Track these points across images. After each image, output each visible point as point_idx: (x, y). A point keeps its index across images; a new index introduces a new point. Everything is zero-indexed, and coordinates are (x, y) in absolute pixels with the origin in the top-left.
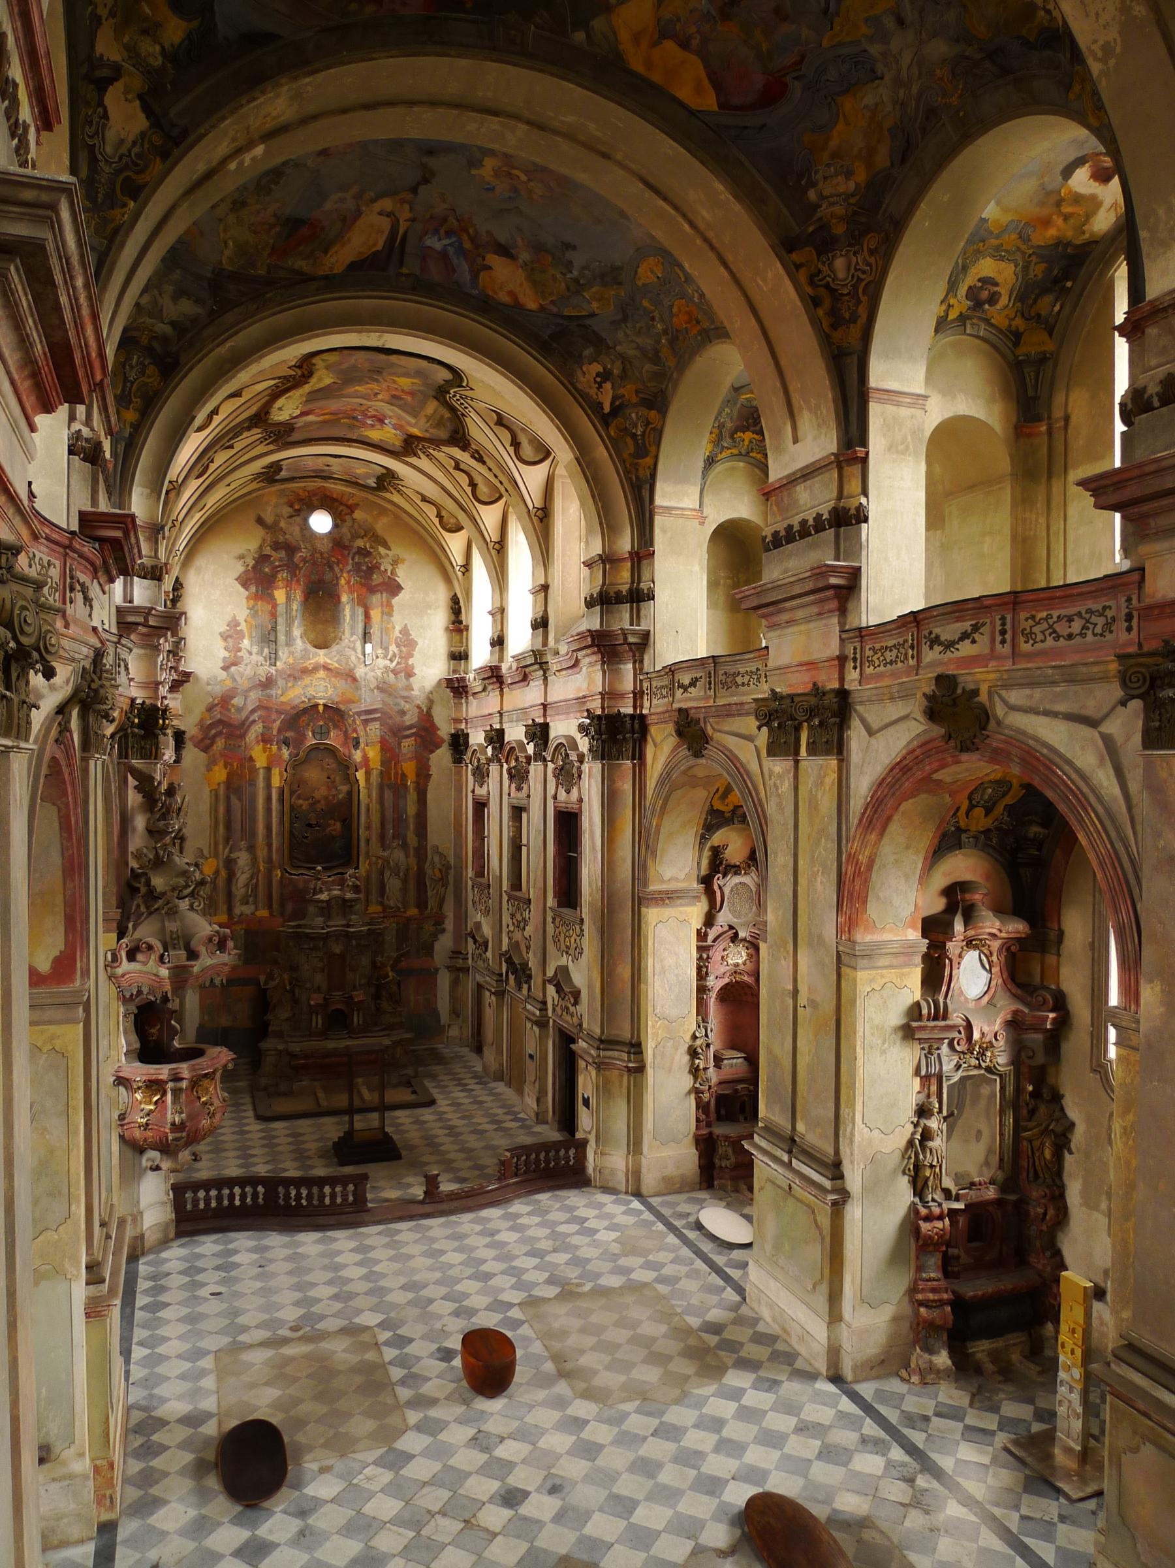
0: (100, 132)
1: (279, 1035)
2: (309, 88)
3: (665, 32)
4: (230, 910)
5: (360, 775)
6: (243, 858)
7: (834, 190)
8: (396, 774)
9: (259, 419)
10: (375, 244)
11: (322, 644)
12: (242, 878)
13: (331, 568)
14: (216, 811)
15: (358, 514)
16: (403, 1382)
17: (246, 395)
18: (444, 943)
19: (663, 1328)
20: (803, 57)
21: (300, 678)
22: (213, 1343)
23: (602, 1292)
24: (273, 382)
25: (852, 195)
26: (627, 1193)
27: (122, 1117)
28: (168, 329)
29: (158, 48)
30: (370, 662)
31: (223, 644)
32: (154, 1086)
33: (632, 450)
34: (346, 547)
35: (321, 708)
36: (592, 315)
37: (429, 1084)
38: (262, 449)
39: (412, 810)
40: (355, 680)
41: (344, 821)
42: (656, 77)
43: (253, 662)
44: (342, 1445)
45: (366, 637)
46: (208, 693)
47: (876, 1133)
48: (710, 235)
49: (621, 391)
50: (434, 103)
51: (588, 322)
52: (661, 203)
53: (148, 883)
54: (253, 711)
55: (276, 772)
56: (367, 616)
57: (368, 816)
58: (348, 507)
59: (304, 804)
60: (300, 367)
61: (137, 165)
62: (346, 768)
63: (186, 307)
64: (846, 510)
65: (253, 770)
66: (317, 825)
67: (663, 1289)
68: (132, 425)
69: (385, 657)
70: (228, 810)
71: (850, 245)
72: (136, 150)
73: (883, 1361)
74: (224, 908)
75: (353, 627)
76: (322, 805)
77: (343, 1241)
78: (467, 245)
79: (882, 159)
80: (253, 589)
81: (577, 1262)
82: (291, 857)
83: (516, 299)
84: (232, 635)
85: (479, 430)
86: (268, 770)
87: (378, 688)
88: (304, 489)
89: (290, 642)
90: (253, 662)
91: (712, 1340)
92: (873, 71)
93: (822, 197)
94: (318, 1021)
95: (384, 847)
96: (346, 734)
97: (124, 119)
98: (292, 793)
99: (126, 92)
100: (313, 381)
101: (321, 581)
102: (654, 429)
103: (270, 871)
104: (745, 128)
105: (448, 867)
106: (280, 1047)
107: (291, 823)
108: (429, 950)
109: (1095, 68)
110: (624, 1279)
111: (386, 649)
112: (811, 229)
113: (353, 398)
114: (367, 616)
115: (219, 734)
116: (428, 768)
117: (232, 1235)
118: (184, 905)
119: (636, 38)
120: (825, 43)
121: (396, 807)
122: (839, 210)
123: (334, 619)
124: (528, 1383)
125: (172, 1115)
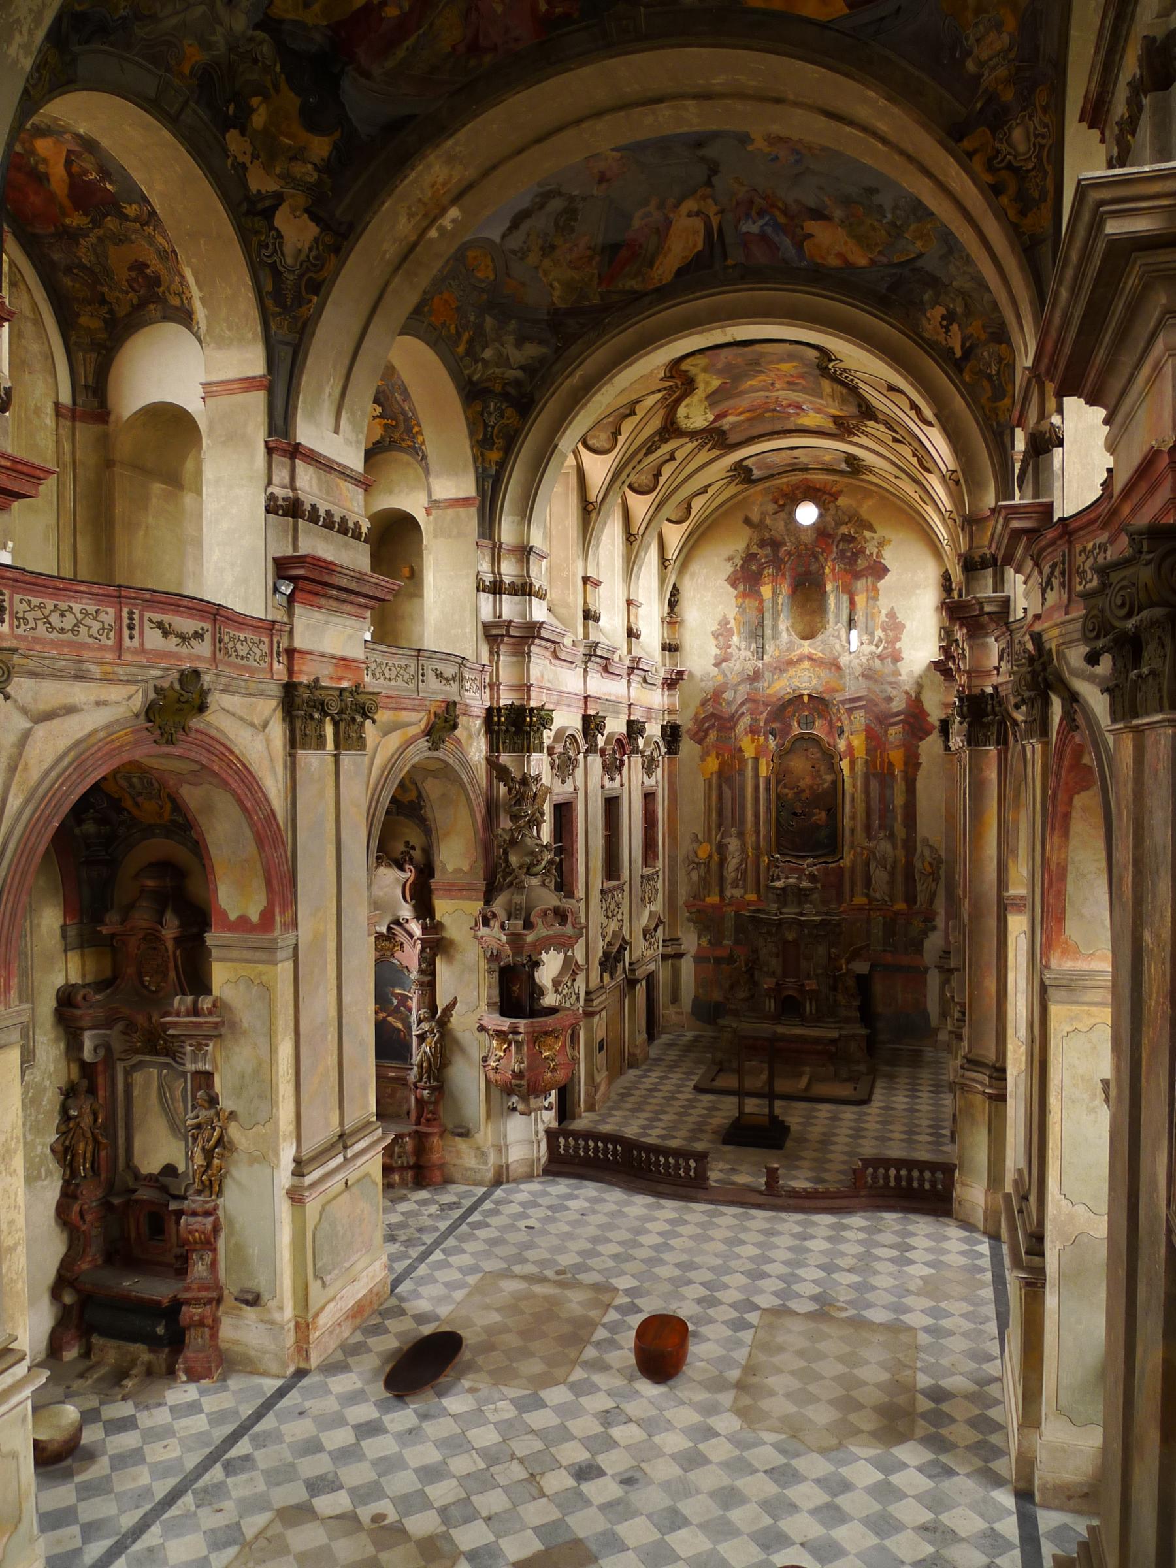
0: (278, 249)
1: (736, 1014)
4: (722, 892)
5: (845, 764)
6: (733, 844)
7: (990, 49)
8: (882, 762)
9: (670, 430)
10: (695, 245)
11: (809, 635)
12: (733, 863)
13: (817, 559)
14: (709, 798)
15: (842, 501)
16: (598, 1344)
17: (641, 410)
18: (934, 942)
19: (884, 1376)
21: (786, 670)
22: (489, 1265)
23: (859, 1323)
24: (660, 395)
25: (1010, 49)
26: (984, 1233)
27: (485, 1059)
28: (519, 374)
29: (310, 166)
30: (854, 647)
31: (714, 642)
32: (500, 1034)
33: (989, 394)
34: (829, 536)
35: (806, 699)
36: (921, 255)
37: (880, 1083)
38: (704, 456)
39: (899, 800)
40: (839, 668)
41: (829, 811)
43: (742, 656)
44: (501, 1376)
45: (851, 624)
46: (702, 689)
47: (1080, 1209)
49: (969, 330)
50: (599, 114)
51: (919, 263)
52: (848, 129)
53: (507, 861)
54: (742, 704)
55: (763, 761)
56: (852, 603)
57: (853, 807)
58: (831, 495)
59: (790, 794)
60: (672, 377)
61: (315, 266)
62: (830, 757)
63: (532, 350)
64: (1043, 434)
65: (743, 761)
66: (803, 814)
67: (923, 1338)
68: (497, 463)
69: (871, 642)
70: (720, 798)
71: (1024, 109)
72: (314, 253)
73: (1086, 1495)
74: (717, 890)
75: (837, 616)
76: (807, 794)
77: (669, 1209)
78: (782, 220)
80: (741, 587)
81: (863, 1287)
82: (778, 844)
83: (846, 260)
84: (722, 633)
85: (878, 400)
86: (756, 759)
87: (863, 675)
88: (787, 484)
89: (776, 635)
90: (742, 656)
91: (924, 1404)
93: (981, 64)
94: (771, 1005)
95: (869, 837)
96: (831, 723)
97: (296, 232)
98: (778, 782)
99: (293, 210)
100: (701, 386)
101: (807, 571)
102: (1007, 365)
103: (758, 857)
104: (882, 19)
105: (938, 861)
106: (734, 1025)
107: (778, 811)
108: (917, 946)
110: (893, 1316)
111: (872, 634)
112: (979, 106)
113: (756, 391)
114: (852, 603)
115: (713, 726)
116: (917, 756)
117: (587, 1183)
118: (535, 881)
121: (882, 798)
122: (1002, 72)
123: (820, 609)
124: (700, 1383)
125: (514, 1063)
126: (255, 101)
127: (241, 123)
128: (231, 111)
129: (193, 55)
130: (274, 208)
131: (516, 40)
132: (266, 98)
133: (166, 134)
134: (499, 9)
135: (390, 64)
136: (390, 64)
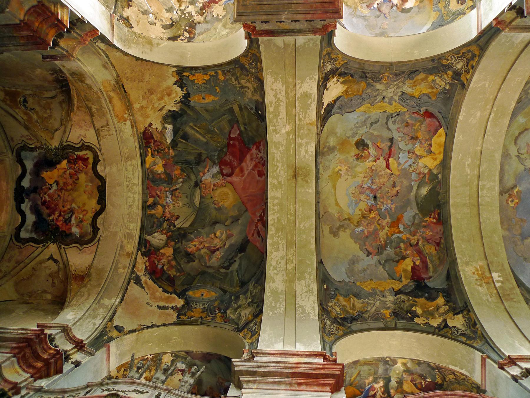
2: (464, 260)
3: (430, 152)
7: (442, 82)
20: (414, 113)
29: (443, 307)
42: (442, 150)
48: (489, 107)
71: (451, 67)
79: (422, 76)
92: (402, 94)
93: (446, 83)
97: (457, 322)
99: (451, 319)
109: (316, 77)
119: (435, 159)
120: (406, 110)
122: (445, 76)
126: (414, 309)
127: (415, 315)
128: (410, 315)
129: (387, 313)
130: (446, 323)
131: (440, 231)
132: (415, 305)
133: (398, 333)
134: (431, 233)
135: (431, 270)
136: (431, 270)
